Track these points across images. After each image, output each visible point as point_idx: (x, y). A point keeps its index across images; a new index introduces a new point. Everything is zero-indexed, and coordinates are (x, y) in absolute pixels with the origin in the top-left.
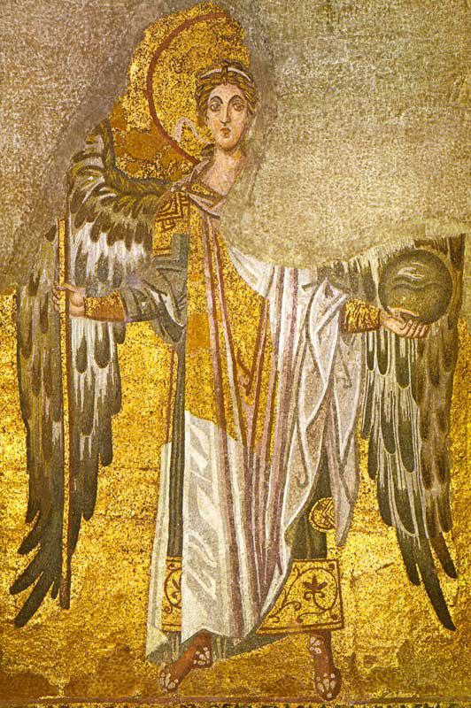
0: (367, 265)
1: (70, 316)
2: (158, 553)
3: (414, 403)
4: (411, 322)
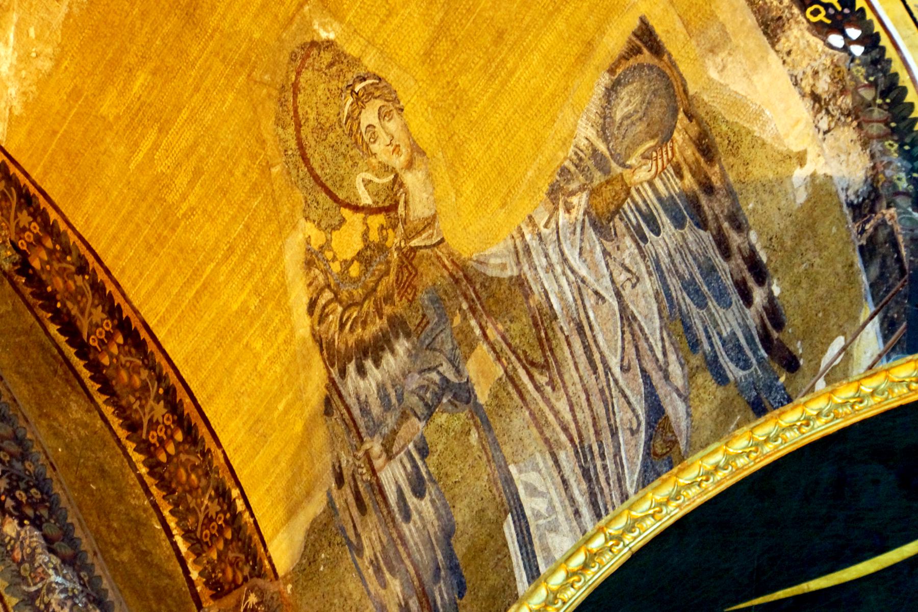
0: (586, 142)
3: (702, 232)
4: (654, 154)
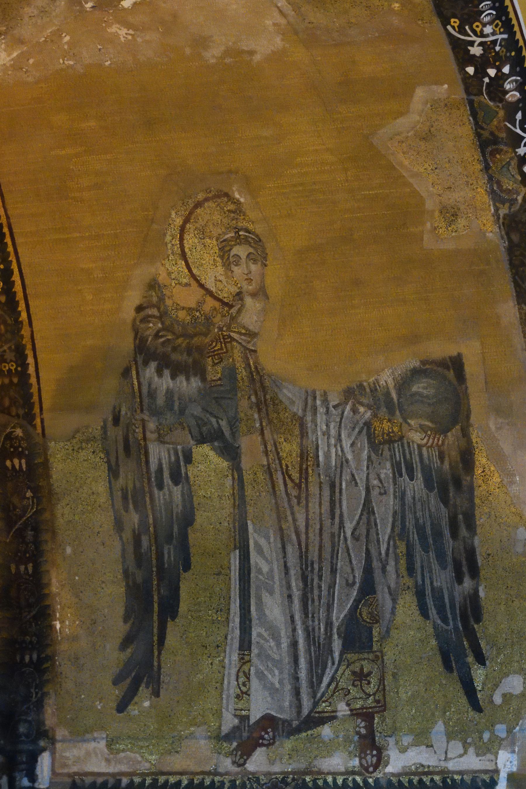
0: (385, 384)
1: (148, 443)
2: (231, 649)
3: (442, 506)
4: (429, 433)
